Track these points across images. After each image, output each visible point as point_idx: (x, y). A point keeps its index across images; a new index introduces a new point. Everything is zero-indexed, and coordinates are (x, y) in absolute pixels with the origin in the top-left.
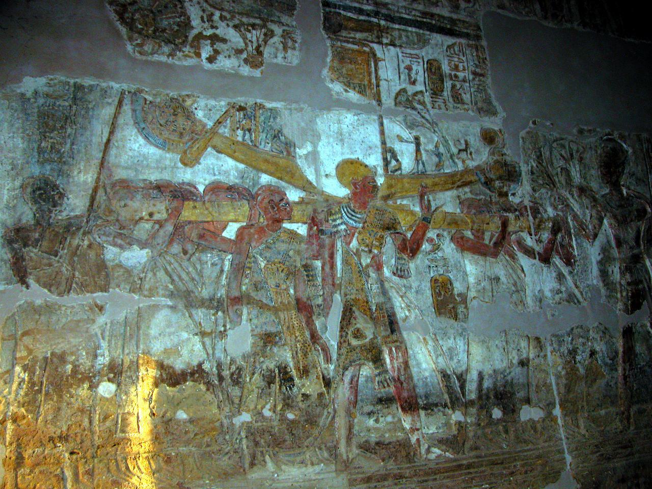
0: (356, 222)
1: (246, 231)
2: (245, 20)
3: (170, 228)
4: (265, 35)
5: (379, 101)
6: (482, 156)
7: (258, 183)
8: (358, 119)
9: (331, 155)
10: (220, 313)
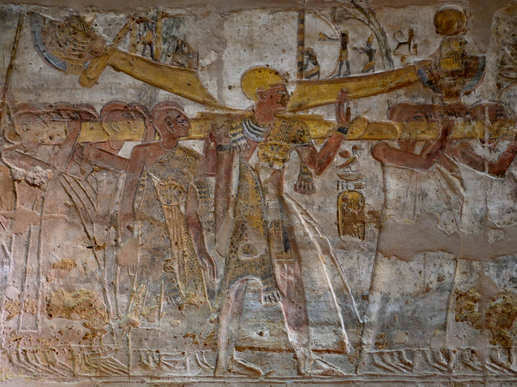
0: (257, 136)
1: (142, 149)
3: (68, 149)
7: (155, 100)
8: (274, 19)
10: (112, 229)
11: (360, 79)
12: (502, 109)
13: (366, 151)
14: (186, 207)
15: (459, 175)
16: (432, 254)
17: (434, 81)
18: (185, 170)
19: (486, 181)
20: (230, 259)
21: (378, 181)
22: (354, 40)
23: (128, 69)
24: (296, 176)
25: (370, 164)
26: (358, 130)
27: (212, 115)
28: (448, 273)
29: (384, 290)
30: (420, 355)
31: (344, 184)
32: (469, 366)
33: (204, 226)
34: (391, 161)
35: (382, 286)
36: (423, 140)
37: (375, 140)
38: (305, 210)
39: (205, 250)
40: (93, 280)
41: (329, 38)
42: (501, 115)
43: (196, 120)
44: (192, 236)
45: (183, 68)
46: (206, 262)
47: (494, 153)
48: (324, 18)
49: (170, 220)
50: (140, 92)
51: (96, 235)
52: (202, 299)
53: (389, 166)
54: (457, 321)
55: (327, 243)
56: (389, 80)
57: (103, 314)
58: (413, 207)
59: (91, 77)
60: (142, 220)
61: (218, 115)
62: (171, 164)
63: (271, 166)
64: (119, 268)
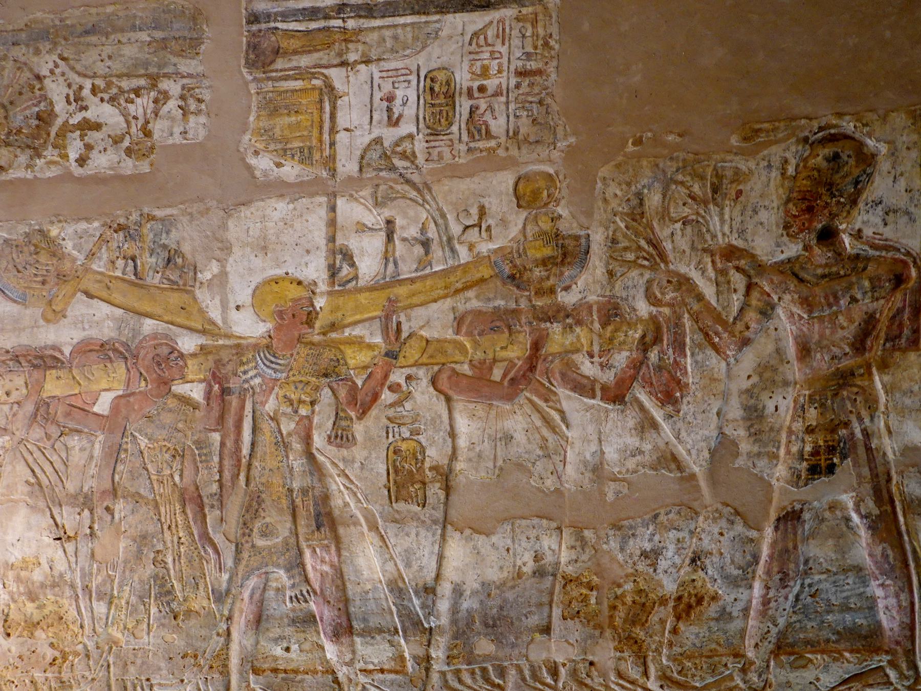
0: (275, 371)
1: (123, 401)
2: (125, 84)
3: (29, 408)
5: (333, 172)
7: (139, 334)
9: (245, 275)
11: (412, 281)
12: (616, 307)
13: (425, 382)
14: (181, 476)
15: (558, 406)
16: (524, 522)
17: (518, 275)
18: (180, 425)
19: (599, 411)
20: (242, 545)
21: (441, 422)
22: (402, 228)
23: (104, 294)
24: (330, 424)
25: (430, 399)
26: (412, 352)
27: (216, 347)
28: (549, 548)
29: (456, 578)
30: (514, 672)
31: (396, 430)
32: (586, 685)
33: (205, 500)
34: (460, 392)
35: (454, 573)
36: (505, 360)
37: (437, 364)
38: (343, 471)
39: (208, 534)
40: (62, 584)
41: (370, 229)
42: (616, 315)
43: (194, 355)
44: (190, 516)
45: (175, 287)
46: (210, 550)
47: (608, 371)
48: (362, 201)
49: (161, 495)
50: (120, 324)
51: (65, 522)
52: (205, 603)
53: (457, 400)
54: (564, 619)
55: (374, 515)
56: (452, 279)
57: (76, 630)
58: (492, 457)
59: (58, 309)
60: (124, 497)
61: (224, 346)
62: (161, 418)
63: (296, 412)
64: (95, 566)
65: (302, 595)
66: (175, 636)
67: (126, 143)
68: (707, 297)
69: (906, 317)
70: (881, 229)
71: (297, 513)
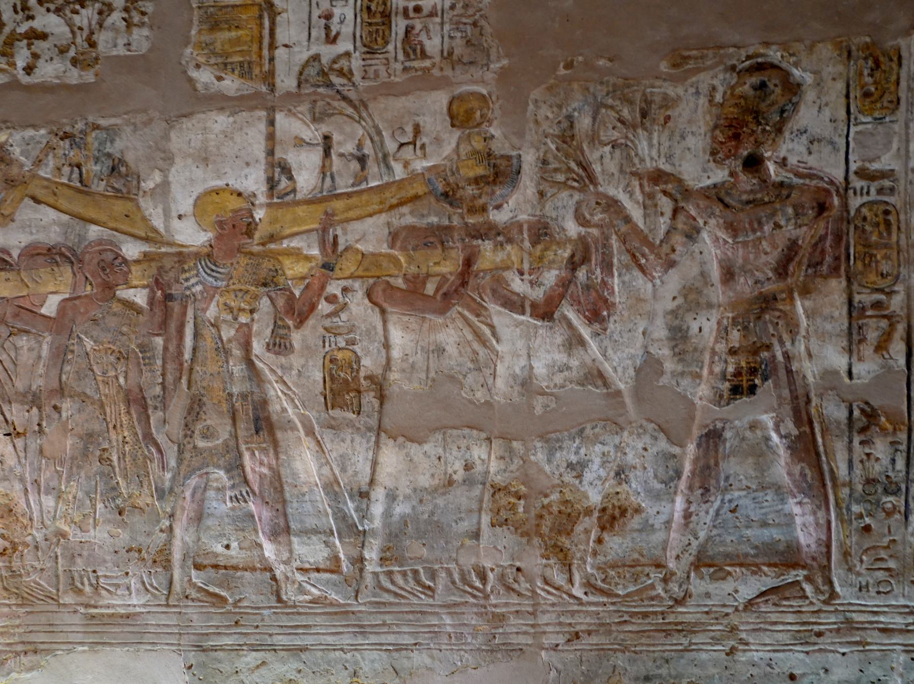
0: (216, 279)
4: (100, 13)
6: (443, 148)
8: (235, 122)
12: (546, 226)
13: (360, 294)
14: (126, 378)
15: (489, 321)
18: (125, 329)
19: (528, 327)
20: (184, 445)
21: (376, 333)
24: (268, 332)
25: (366, 311)
26: (349, 265)
27: (158, 254)
31: (332, 339)
33: (149, 402)
34: (393, 305)
36: (438, 275)
37: (372, 277)
38: (281, 377)
39: (152, 434)
40: (12, 477)
42: (546, 234)
43: (137, 262)
44: (135, 416)
45: (120, 195)
46: (153, 450)
47: (537, 289)
49: (106, 396)
51: (14, 419)
53: (392, 313)
55: (310, 421)
57: (25, 522)
58: (425, 368)
60: (71, 397)
61: (166, 254)
62: (107, 321)
63: (236, 319)
64: (44, 461)
65: (242, 495)
66: (120, 531)
67: (72, 53)
68: (635, 219)
69: (828, 243)
70: (806, 158)
71: (237, 418)
